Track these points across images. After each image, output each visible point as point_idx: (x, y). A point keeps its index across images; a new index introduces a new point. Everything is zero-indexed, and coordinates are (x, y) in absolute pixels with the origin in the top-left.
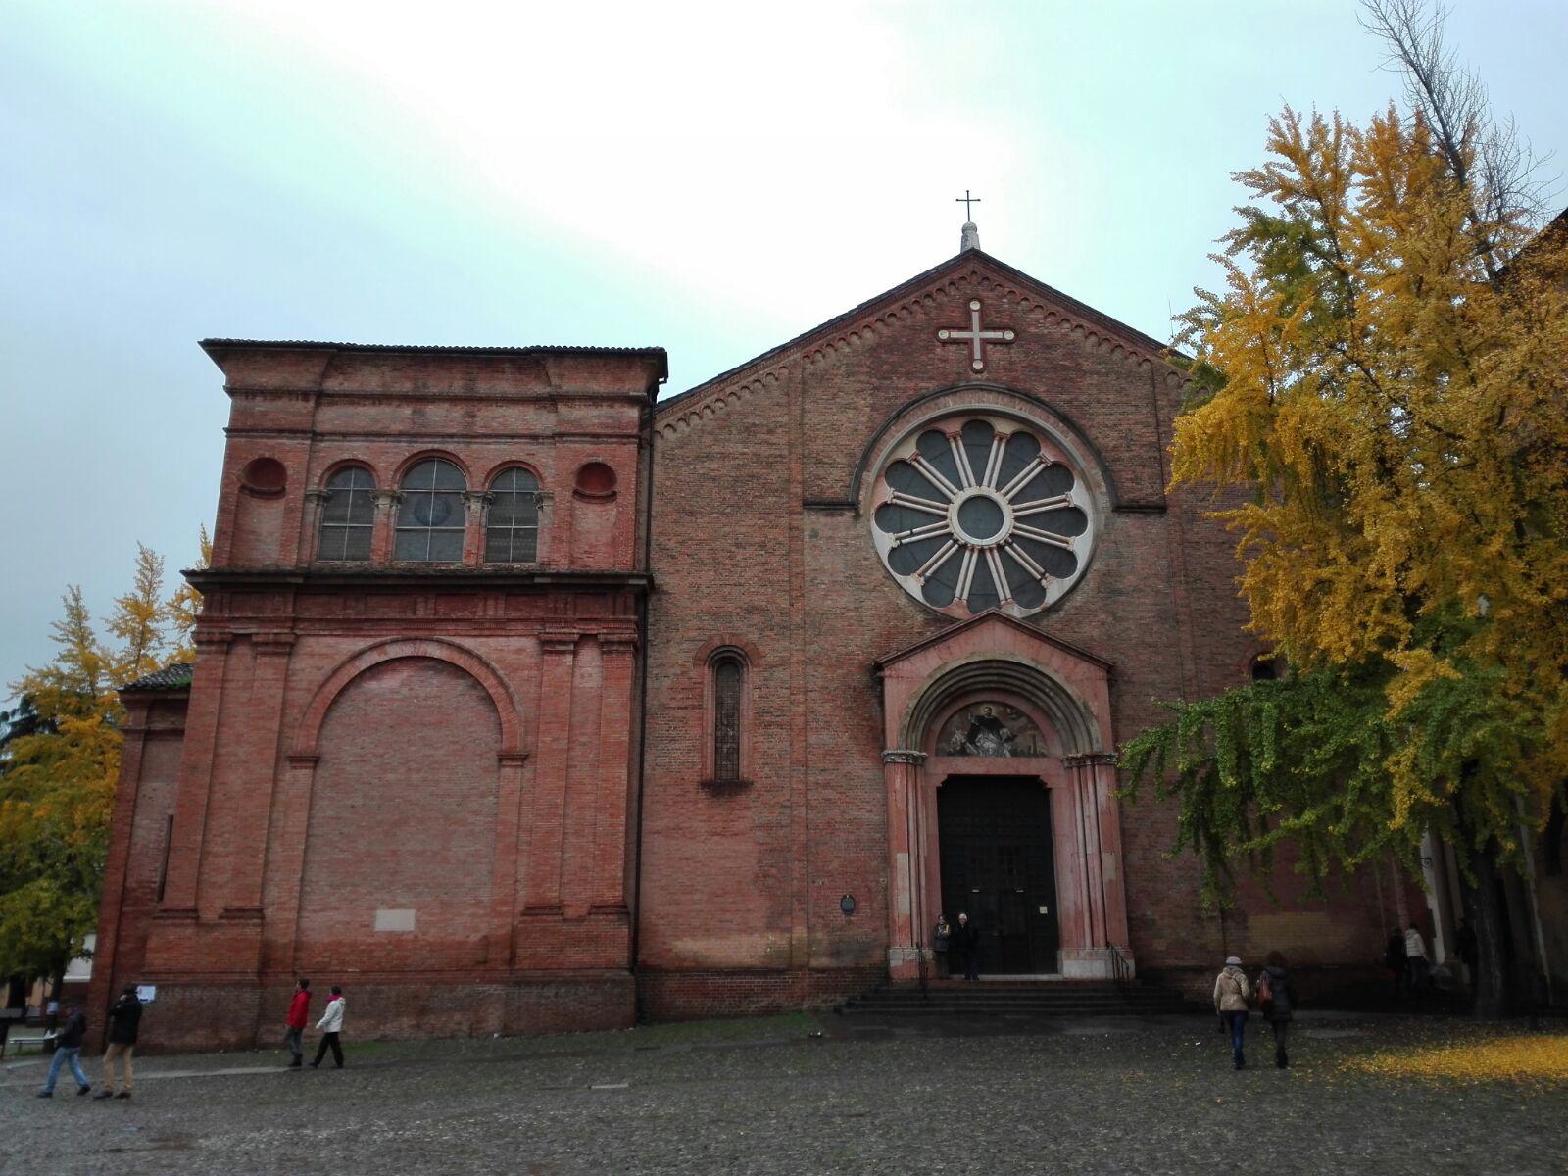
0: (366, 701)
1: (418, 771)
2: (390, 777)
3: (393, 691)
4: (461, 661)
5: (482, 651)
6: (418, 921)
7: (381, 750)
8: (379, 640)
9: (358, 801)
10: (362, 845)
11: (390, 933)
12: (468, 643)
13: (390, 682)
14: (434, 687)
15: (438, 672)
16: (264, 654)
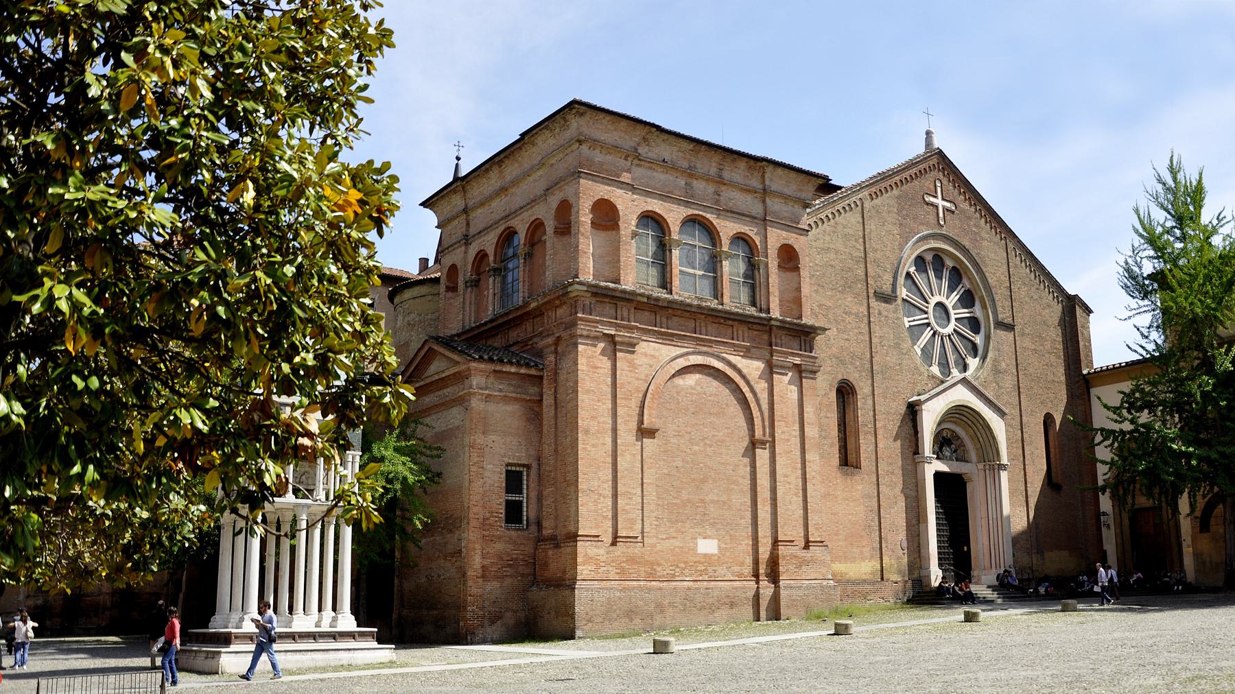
0: (678, 393)
1: (711, 446)
2: (696, 448)
3: (692, 388)
4: (729, 372)
5: (739, 366)
6: (719, 547)
7: (689, 429)
8: (685, 350)
9: (680, 464)
10: (684, 495)
11: (705, 555)
12: (735, 359)
13: (692, 379)
14: (714, 385)
15: (715, 378)
16: (621, 351)
